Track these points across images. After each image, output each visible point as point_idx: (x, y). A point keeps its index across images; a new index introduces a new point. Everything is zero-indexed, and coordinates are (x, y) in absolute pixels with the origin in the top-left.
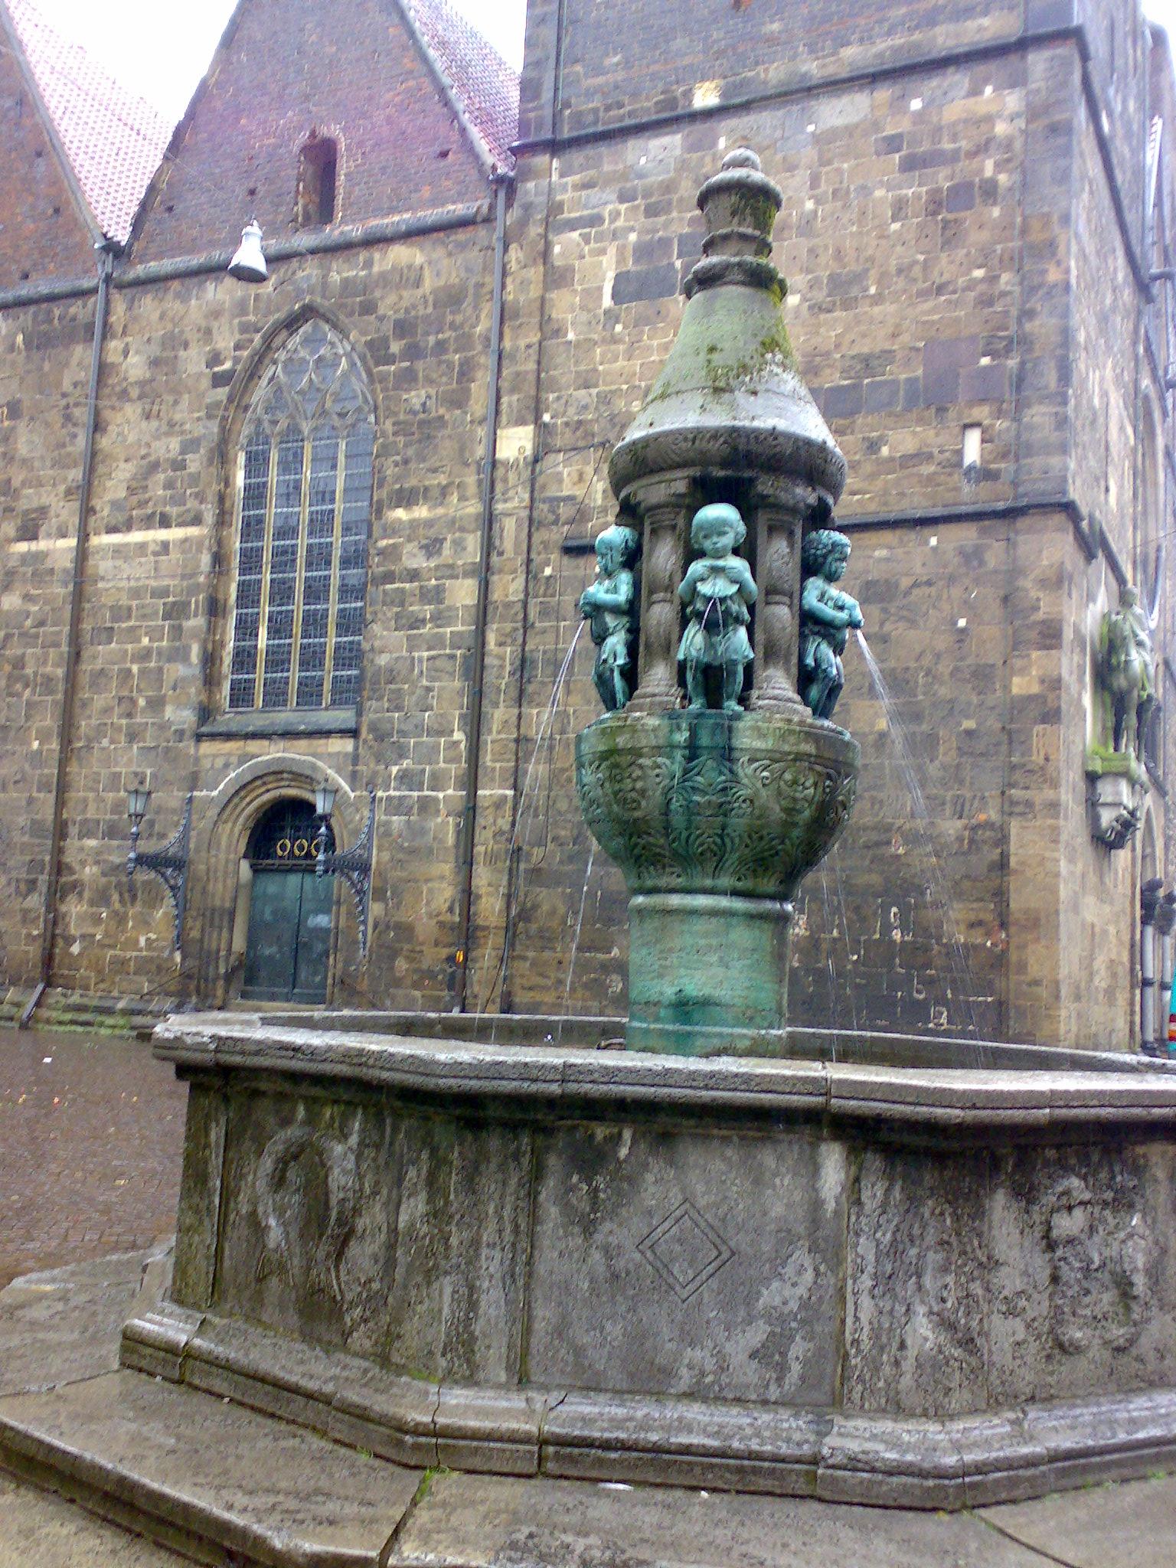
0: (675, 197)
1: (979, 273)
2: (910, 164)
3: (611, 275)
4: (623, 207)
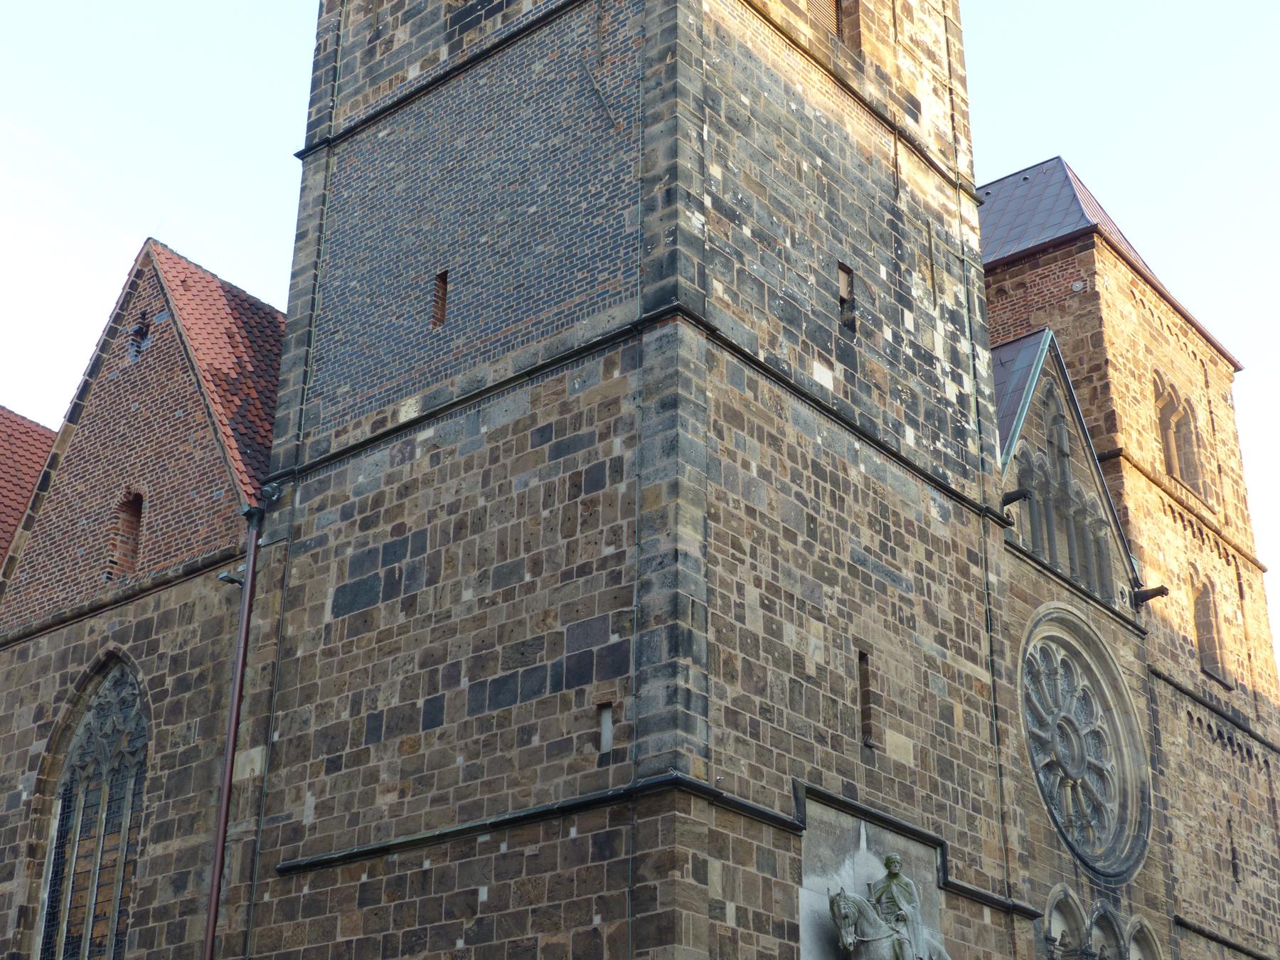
0: (382, 510)
1: (609, 551)
2: (558, 452)
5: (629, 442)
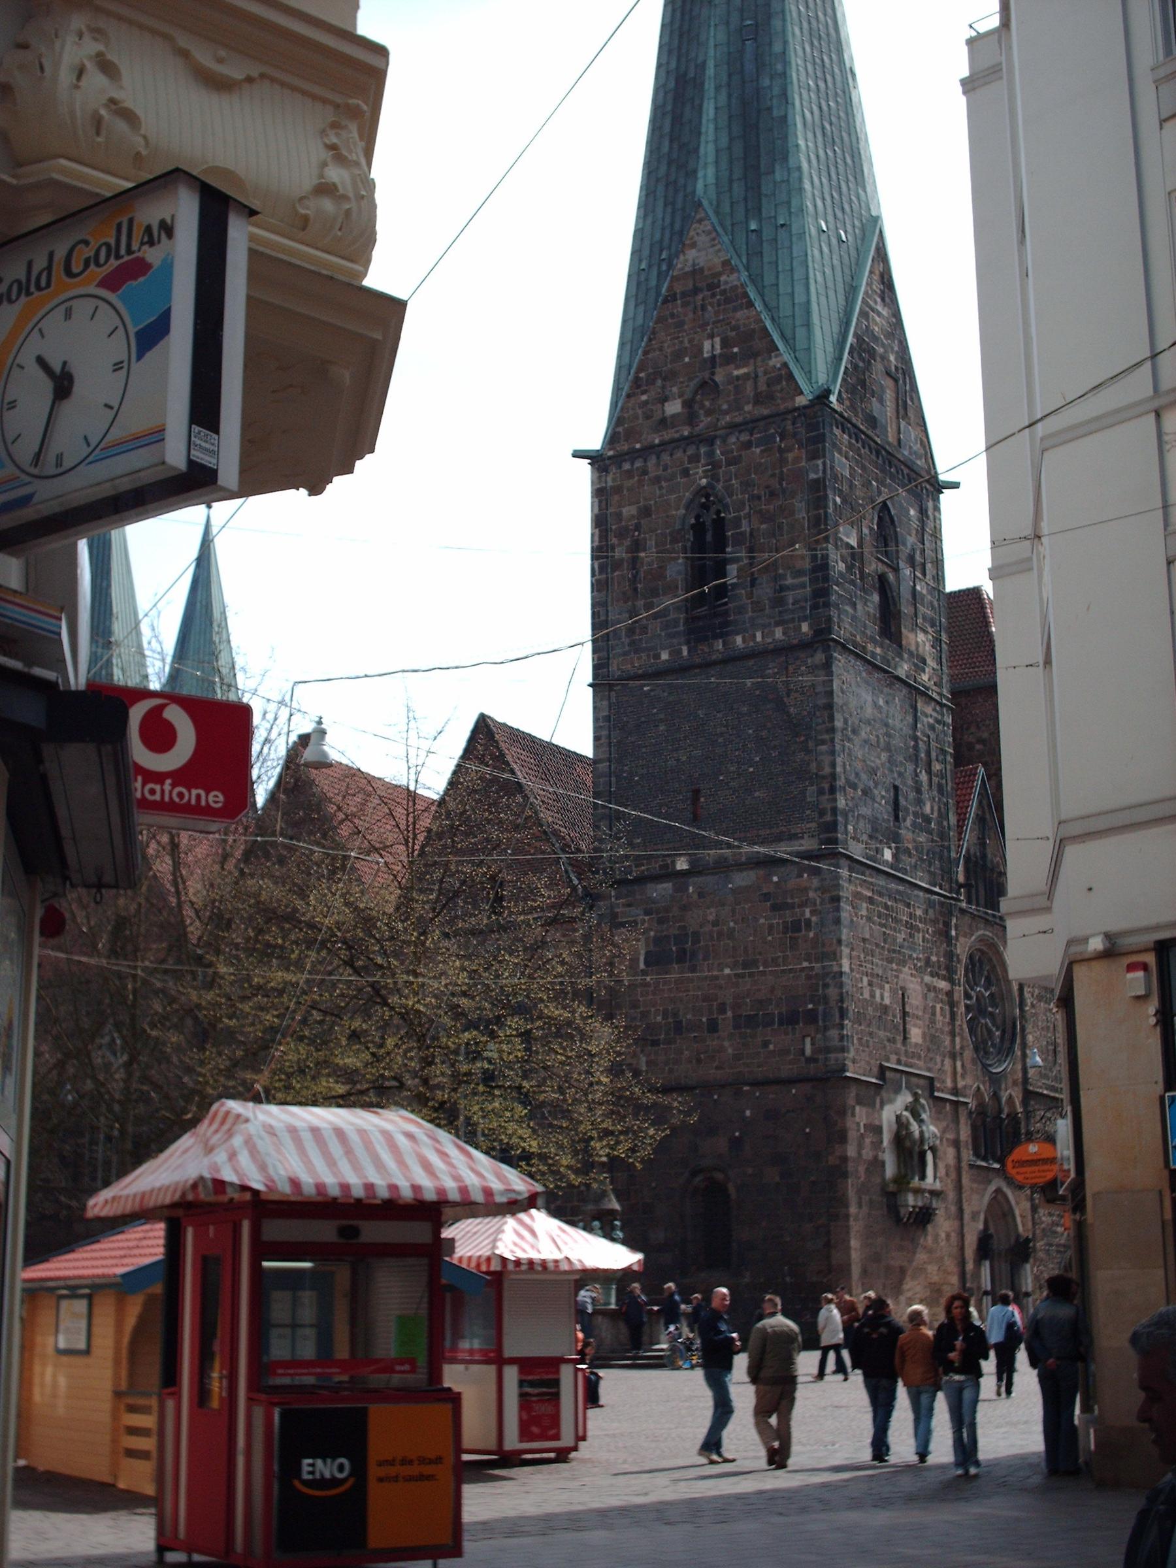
1: (805, 964)
2: (775, 908)
3: (643, 952)
4: (646, 918)
5: (813, 913)
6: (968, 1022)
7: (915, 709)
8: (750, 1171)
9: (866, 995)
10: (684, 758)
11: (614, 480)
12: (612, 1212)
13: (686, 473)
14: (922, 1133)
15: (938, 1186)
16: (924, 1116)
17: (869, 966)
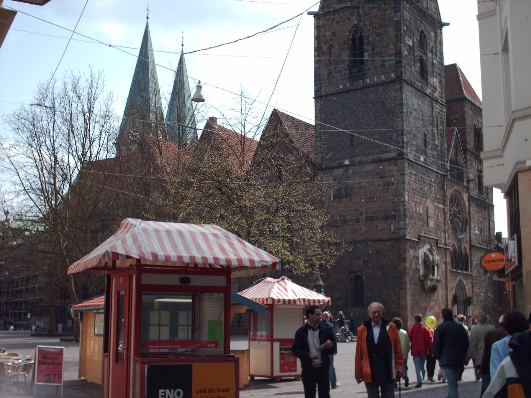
1: (392, 198)
2: (381, 178)
3: (332, 194)
6: (451, 220)
7: (433, 106)
8: (371, 272)
9: (414, 209)
10: (348, 124)
11: (323, 23)
12: (321, 286)
13: (349, 19)
14: (433, 259)
15: (439, 278)
16: (434, 253)
17: (415, 199)
